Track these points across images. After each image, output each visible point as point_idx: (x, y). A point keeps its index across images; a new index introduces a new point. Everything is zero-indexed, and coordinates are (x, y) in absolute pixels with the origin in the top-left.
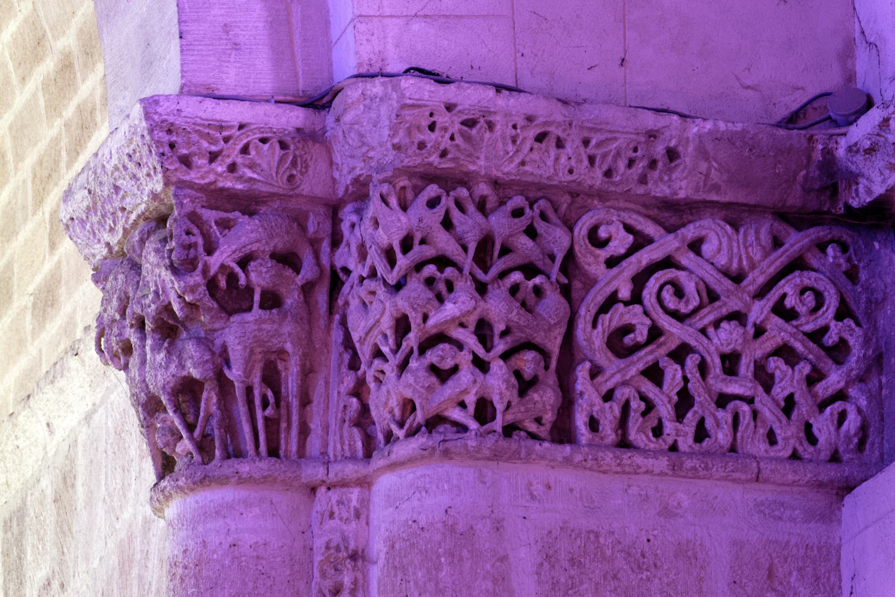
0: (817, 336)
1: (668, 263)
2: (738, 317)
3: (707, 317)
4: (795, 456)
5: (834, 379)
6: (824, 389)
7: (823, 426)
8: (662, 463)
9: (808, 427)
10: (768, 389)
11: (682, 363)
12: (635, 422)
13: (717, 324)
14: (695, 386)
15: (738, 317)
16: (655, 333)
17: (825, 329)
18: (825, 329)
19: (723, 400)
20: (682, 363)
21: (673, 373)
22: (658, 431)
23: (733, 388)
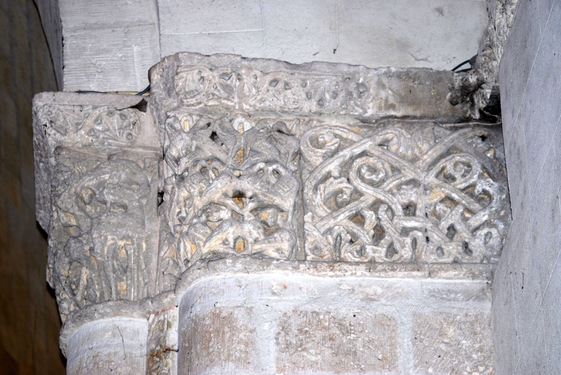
0: (469, 190)
1: (364, 154)
2: (414, 182)
3: (391, 184)
4: (455, 262)
5: (483, 216)
6: (474, 222)
7: (477, 244)
8: (361, 269)
9: (466, 246)
10: (437, 225)
11: (376, 211)
12: (346, 247)
13: (399, 187)
14: (385, 224)
15: (414, 182)
16: (357, 194)
17: (473, 186)
18: (473, 186)
19: (405, 232)
20: (376, 211)
21: (369, 214)
22: (361, 252)
23: (410, 223)
